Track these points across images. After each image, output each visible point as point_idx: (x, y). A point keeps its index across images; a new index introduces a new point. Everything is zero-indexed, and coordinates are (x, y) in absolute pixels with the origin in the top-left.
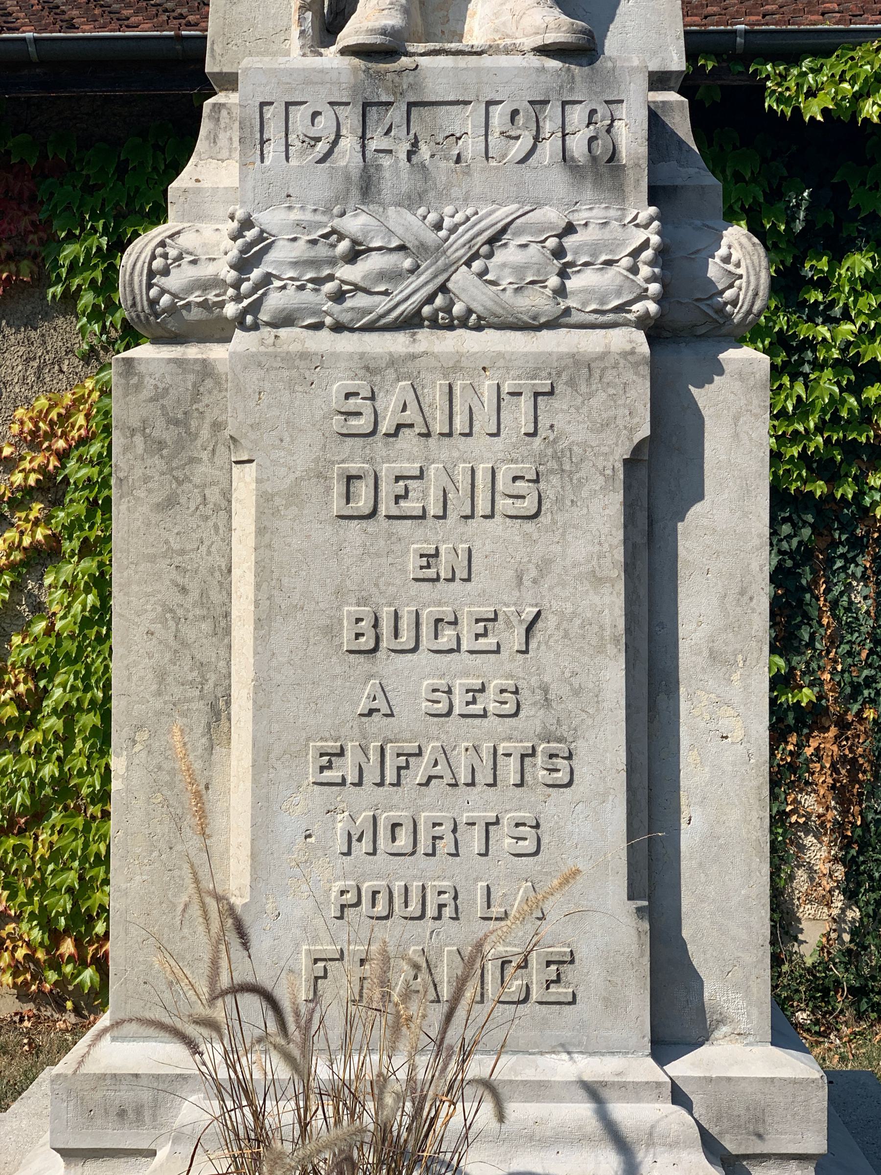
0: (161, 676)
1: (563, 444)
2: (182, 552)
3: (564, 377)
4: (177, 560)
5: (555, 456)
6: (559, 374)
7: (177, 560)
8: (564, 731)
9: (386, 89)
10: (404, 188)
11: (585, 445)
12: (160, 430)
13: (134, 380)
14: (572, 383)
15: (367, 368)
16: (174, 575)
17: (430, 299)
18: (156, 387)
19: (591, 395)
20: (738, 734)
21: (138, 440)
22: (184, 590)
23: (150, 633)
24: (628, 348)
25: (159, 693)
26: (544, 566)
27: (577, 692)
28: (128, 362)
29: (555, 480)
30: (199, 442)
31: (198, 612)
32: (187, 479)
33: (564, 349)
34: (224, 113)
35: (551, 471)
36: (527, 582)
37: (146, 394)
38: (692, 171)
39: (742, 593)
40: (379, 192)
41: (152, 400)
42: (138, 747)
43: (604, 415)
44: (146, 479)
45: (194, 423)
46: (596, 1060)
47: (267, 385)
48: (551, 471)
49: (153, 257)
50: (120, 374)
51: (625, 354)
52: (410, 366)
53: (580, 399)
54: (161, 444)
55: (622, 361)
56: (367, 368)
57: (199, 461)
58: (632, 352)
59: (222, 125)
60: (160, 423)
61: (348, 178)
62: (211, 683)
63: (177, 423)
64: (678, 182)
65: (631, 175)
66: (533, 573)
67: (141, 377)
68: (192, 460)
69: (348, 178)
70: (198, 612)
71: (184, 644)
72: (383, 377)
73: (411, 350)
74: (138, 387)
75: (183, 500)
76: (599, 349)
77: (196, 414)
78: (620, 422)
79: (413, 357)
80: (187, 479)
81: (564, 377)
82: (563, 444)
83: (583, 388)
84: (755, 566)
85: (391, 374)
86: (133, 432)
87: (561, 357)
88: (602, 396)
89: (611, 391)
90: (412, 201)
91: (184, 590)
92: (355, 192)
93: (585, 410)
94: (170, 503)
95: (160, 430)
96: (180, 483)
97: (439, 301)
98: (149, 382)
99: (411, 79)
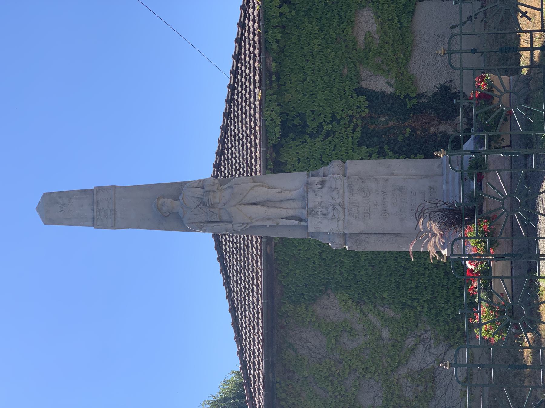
12: (358, 244)
90: (327, 209)
94: (368, 242)
95: (358, 244)
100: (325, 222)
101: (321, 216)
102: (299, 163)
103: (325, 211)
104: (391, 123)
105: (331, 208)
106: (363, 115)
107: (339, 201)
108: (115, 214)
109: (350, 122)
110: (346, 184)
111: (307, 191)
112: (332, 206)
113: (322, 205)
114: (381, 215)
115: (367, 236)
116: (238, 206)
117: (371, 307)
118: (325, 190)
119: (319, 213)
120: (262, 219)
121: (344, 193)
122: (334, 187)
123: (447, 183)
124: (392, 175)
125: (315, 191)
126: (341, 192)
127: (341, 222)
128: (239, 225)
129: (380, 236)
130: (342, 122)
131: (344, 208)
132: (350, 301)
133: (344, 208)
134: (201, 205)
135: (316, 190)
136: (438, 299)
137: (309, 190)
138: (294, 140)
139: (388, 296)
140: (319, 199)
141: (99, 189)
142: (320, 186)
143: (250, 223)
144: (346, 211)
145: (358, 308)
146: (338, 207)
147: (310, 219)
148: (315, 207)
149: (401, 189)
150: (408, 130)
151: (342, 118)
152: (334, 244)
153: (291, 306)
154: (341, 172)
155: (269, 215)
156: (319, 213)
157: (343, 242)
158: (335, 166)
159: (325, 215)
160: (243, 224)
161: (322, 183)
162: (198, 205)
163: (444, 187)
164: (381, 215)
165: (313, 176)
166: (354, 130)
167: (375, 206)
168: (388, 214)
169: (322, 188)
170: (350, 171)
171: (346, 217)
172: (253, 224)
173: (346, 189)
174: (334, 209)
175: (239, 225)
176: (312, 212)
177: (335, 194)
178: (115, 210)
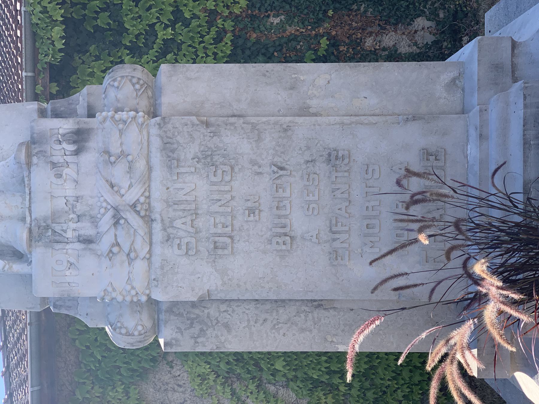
0: (302, 330)
1: (199, 155)
2: (249, 320)
3: (170, 154)
4: (252, 323)
5: (205, 158)
6: (169, 157)
7: (252, 323)
8: (325, 154)
9: (46, 232)
10: (89, 224)
11: (200, 145)
13: (174, 341)
14: (173, 151)
15: (167, 240)
16: (258, 325)
17: (138, 213)
18: (177, 332)
19: (178, 143)
20: (327, 76)
21: (199, 340)
22: (265, 320)
23: (284, 335)
24: (157, 126)
25: (310, 331)
26: (253, 163)
27: (308, 148)
28: (166, 344)
29: (216, 158)
30: (201, 314)
31: (274, 314)
32: (216, 319)
33: (159, 155)
34: (57, 303)
35: (212, 159)
36: (260, 170)
37: (179, 336)
38: (81, 99)
39: (264, 75)
40: (91, 236)
41: (182, 334)
42: (334, 340)
43: (187, 136)
44: (217, 336)
45: (193, 316)
46: (470, 138)
47: (175, 284)
48: (212, 159)
49: (121, 333)
50: (171, 348)
51: (160, 128)
52: (167, 222)
53: (180, 147)
54: (202, 330)
55: (163, 129)
56: (167, 240)
57: (208, 313)
58: (159, 124)
59: (63, 304)
60: (192, 330)
61: (84, 249)
62: (306, 308)
63: (192, 323)
64: (86, 104)
65: (82, 126)
66: (256, 167)
67: (172, 339)
68: (208, 317)
69: (84, 249)
70: (274, 314)
71: (289, 320)
72: (172, 234)
73: (159, 221)
74: (177, 340)
75: (226, 321)
76: (158, 139)
77: (188, 315)
78: (190, 130)
79: (162, 220)
80: (216, 319)
81: (170, 154)
82: (199, 155)
83: (175, 146)
84: (253, 70)
85: (170, 230)
86: (196, 342)
87: (162, 156)
88: (179, 138)
89: (176, 134)
90: (94, 221)
93: (185, 146)
94: (227, 326)
95: (195, 330)
96: (218, 322)
98: (174, 335)
99: (42, 222)
100: (89, 262)
103: (87, 229)
104: (291, 30)
105: (106, 221)
106: (237, 11)
109: (211, 24)
110: (156, 143)
111: (29, 164)
112: (111, 213)
113: (80, 208)
114: (270, 242)
115: (223, 307)
117: (252, 387)
118: (89, 158)
119: (69, 234)
121: (150, 169)
122: (115, 149)
123: (482, 137)
124: (304, 111)
125: (54, 165)
126: (141, 165)
127: (140, 266)
129: (268, 306)
130: (194, 23)
132: (212, 377)
133: (148, 220)
135: (58, 158)
136: (380, 370)
137: (35, 160)
138: (98, 58)
139: (284, 367)
140: (69, 190)
142: (72, 148)
144: (157, 227)
145: (228, 390)
146: (131, 216)
147: (38, 253)
148: (55, 216)
149: (334, 158)
150: (324, 42)
151: (195, 16)
152: (126, 332)
153: (96, 387)
154: (144, 103)
156: (69, 234)
157: (148, 324)
158: (123, 83)
159: (87, 241)
161: (79, 138)
163: (472, 150)
164: (270, 242)
165: (57, 115)
166: (218, 40)
167: (251, 211)
168: (292, 238)
169: (77, 153)
170: (168, 100)
171: (158, 250)
173: (157, 159)
174: (116, 224)
176: (44, 232)
177: (118, 173)
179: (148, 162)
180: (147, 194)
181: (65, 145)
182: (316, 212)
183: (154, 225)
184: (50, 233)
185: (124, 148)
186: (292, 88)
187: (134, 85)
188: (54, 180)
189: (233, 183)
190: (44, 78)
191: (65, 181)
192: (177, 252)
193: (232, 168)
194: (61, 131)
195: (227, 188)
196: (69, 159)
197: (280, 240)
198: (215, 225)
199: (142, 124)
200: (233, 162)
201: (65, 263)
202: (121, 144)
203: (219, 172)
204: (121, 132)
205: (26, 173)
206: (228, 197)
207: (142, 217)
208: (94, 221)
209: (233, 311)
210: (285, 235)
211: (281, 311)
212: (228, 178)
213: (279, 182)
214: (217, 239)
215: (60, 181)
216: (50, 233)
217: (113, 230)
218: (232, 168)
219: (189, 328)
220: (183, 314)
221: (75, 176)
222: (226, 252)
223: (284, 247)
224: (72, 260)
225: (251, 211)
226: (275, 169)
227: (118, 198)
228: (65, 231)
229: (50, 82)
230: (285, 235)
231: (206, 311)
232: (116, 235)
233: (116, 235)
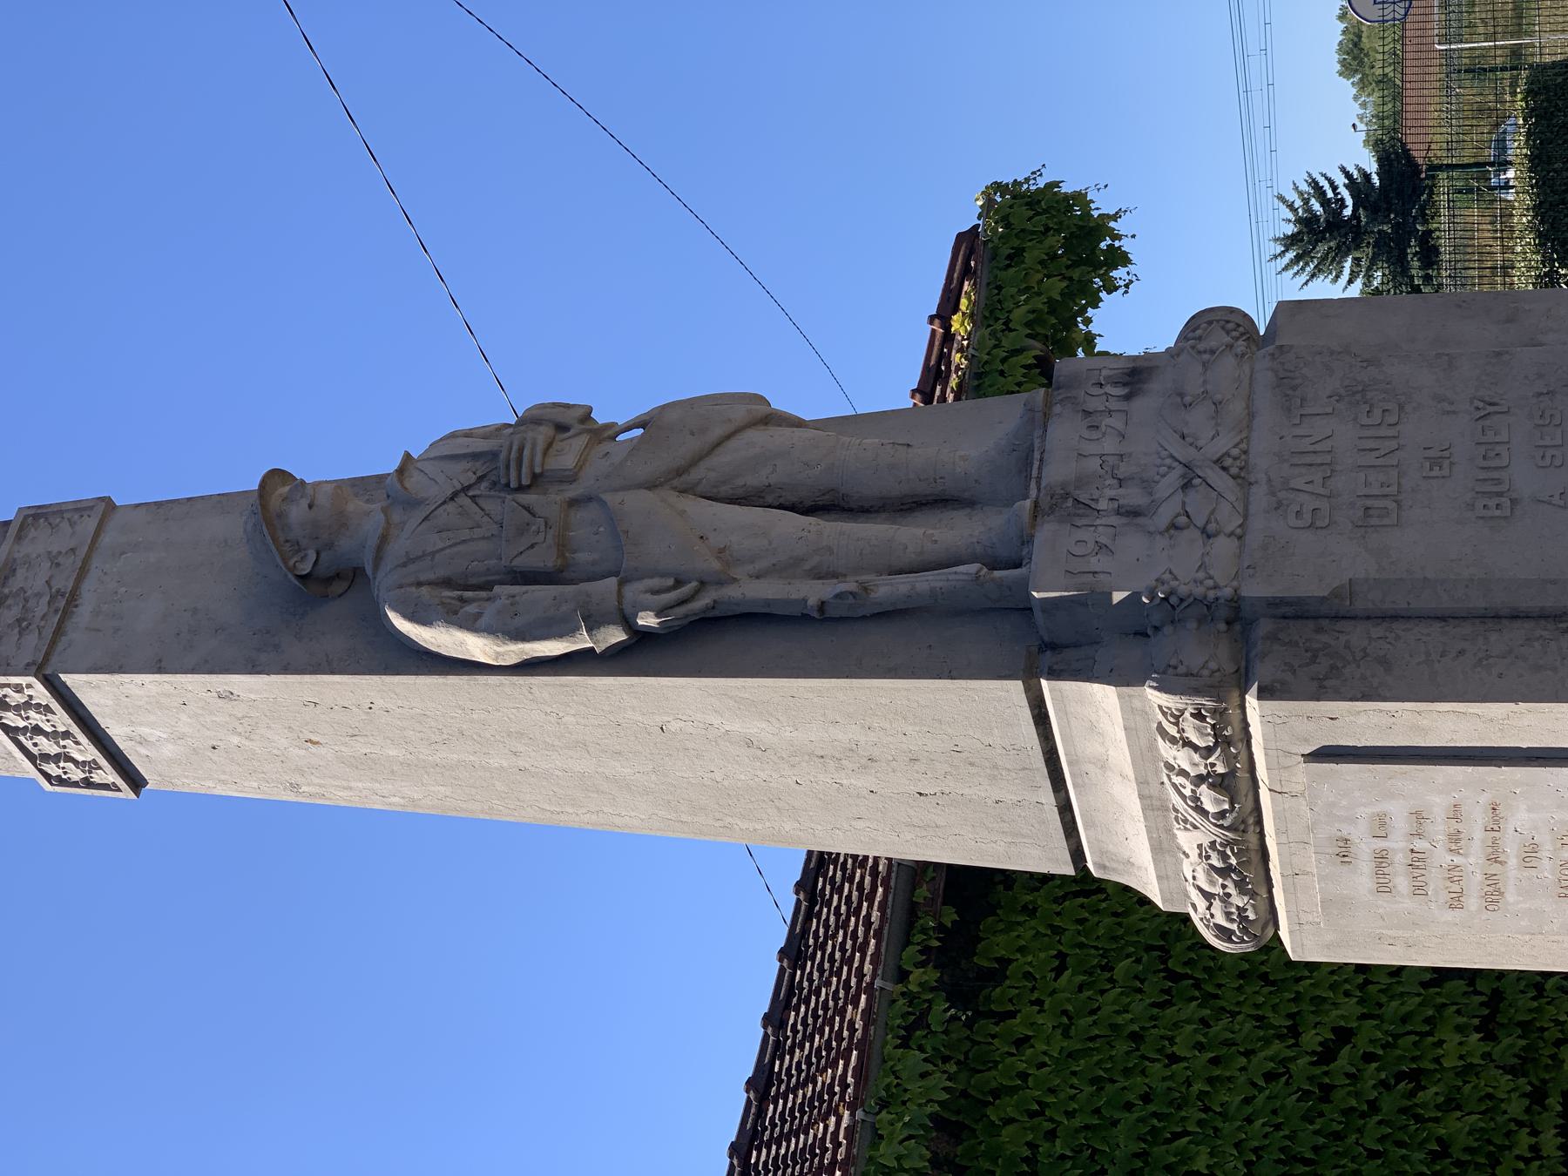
1: (1342, 391)
14: (1294, 388)
21: (1326, 683)
22: (1461, 652)
23: (1500, 676)
27: (1540, 376)
29: (1369, 395)
32: (1364, 650)
36: (1452, 408)
45: (1315, 646)
54: (1333, 667)
57: (1347, 642)
63: (1315, 657)
68: (1347, 646)
79: (1269, 480)
80: (1364, 650)
90: (1147, 485)
91: (1461, 652)
92: (1140, 520)
94: (1385, 663)
96: (1367, 655)
97: (1228, 462)
100: (1132, 544)
101: (1114, 520)
102: (1059, 971)
103: (1133, 496)
107: (1224, 443)
108: (66, 614)
112: (1179, 470)
113: (1124, 470)
114: (1471, 507)
115: (1377, 631)
116: (673, 497)
119: (1103, 505)
120: (787, 568)
121: (1251, 415)
125: (1087, 413)
126: (1237, 408)
127: (1223, 547)
128: (655, 582)
129: (1467, 628)
131: (1243, 479)
133: (1243, 479)
134: (484, 485)
135: (1094, 404)
137: (1057, 409)
140: (1109, 445)
141: (35, 517)
143: (720, 584)
144: (1259, 495)
148: (1081, 482)
155: (830, 549)
157: (1230, 668)
159: (1134, 513)
160: (679, 583)
162: (465, 489)
164: (1471, 507)
167: (1436, 462)
168: (1514, 502)
169: (1127, 398)
172: (732, 592)
175: (655, 582)
177: (1198, 420)
178: (73, 598)
179: (1249, 398)
180: (1243, 446)
181: (1109, 389)
182: (1558, 462)
183: (1254, 489)
184: (1070, 502)
185: (1209, 387)
186: (1509, 320)
187: (1228, 333)
188: (1086, 434)
189: (1398, 428)
190: (933, 879)
191: (1104, 434)
192: (1293, 521)
193: (1401, 407)
194: (1104, 372)
195: (1391, 432)
196: (1114, 405)
197: (1492, 503)
198: (1367, 484)
199: (1243, 355)
200: (1403, 398)
201: (1091, 545)
202: (1205, 382)
203: (1377, 412)
204: (1205, 364)
205: (1038, 433)
206: (1393, 444)
207: (1234, 478)
208: (1147, 485)
209: (1398, 638)
210: (1500, 494)
211: (1493, 637)
212: (1393, 419)
213: (1487, 422)
214: (1369, 503)
215: (1095, 435)
216: (1070, 502)
217: (1179, 496)
218: (1401, 407)
219: (1308, 665)
220: (1297, 644)
221: (1119, 425)
222: (1386, 521)
223: (1498, 513)
224: (1103, 540)
225: (1436, 462)
226: (1481, 405)
227: (1192, 450)
228: (1096, 501)
229: (944, 904)
230: (1500, 494)
231: (1343, 638)
232: (1184, 503)
233: (1184, 503)
